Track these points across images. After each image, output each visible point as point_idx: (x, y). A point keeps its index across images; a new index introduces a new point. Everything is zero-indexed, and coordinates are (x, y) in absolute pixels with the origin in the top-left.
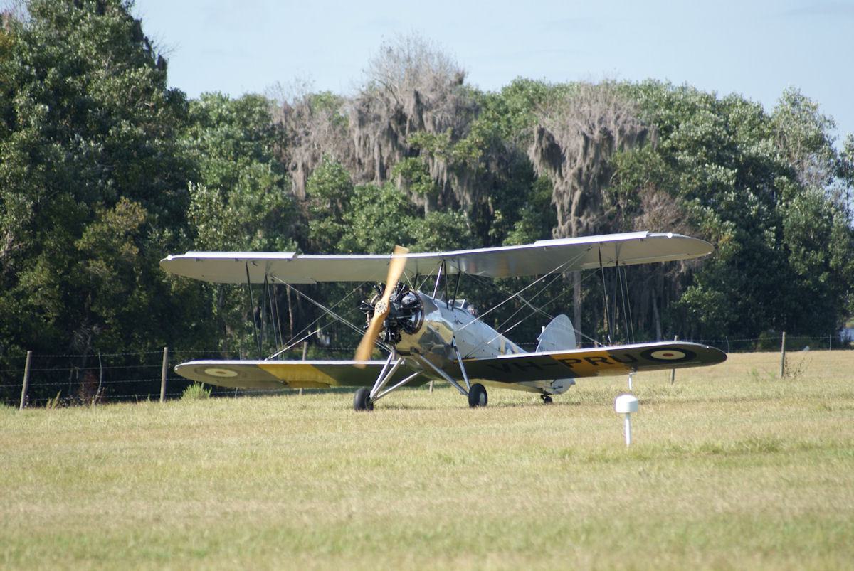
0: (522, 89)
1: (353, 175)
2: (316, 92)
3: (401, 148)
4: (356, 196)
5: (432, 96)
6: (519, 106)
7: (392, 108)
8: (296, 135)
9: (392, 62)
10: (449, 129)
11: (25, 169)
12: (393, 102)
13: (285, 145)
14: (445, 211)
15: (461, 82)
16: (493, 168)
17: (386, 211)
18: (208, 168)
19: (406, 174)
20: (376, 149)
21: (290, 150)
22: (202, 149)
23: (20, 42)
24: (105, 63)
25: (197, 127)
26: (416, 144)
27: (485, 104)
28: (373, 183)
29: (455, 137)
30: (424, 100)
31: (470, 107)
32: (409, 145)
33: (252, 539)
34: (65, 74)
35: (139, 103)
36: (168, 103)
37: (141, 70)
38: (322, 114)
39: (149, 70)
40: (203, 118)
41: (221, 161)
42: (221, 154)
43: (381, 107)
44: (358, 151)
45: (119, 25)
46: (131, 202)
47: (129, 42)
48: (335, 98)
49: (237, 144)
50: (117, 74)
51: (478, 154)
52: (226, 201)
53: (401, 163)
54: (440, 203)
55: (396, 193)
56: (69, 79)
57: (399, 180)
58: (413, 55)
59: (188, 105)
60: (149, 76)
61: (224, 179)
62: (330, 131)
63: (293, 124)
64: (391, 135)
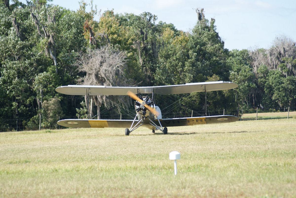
1: (269, 68)
2: (260, 48)
4: (269, 73)
5: (288, 49)
8: (255, 58)
10: (292, 57)
12: (278, 50)
13: (253, 61)
14: (291, 76)
15: (295, 45)
17: (277, 76)
18: (234, 67)
21: (253, 62)
22: (233, 63)
25: (231, 57)
26: (284, 60)
30: (286, 50)
32: (282, 60)
33: (245, 154)
35: (218, 52)
36: (224, 52)
39: (220, 44)
40: (233, 55)
41: (237, 65)
42: (237, 64)
44: (270, 62)
45: (213, 34)
47: (215, 38)
48: (264, 50)
49: (240, 61)
50: (212, 45)
52: (238, 74)
53: (280, 65)
55: (279, 72)
56: (202, 47)
57: (280, 69)
59: (229, 52)
60: (220, 46)
61: (238, 69)
62: (263, 57)
63: (254, 56)
64: (278, 58)
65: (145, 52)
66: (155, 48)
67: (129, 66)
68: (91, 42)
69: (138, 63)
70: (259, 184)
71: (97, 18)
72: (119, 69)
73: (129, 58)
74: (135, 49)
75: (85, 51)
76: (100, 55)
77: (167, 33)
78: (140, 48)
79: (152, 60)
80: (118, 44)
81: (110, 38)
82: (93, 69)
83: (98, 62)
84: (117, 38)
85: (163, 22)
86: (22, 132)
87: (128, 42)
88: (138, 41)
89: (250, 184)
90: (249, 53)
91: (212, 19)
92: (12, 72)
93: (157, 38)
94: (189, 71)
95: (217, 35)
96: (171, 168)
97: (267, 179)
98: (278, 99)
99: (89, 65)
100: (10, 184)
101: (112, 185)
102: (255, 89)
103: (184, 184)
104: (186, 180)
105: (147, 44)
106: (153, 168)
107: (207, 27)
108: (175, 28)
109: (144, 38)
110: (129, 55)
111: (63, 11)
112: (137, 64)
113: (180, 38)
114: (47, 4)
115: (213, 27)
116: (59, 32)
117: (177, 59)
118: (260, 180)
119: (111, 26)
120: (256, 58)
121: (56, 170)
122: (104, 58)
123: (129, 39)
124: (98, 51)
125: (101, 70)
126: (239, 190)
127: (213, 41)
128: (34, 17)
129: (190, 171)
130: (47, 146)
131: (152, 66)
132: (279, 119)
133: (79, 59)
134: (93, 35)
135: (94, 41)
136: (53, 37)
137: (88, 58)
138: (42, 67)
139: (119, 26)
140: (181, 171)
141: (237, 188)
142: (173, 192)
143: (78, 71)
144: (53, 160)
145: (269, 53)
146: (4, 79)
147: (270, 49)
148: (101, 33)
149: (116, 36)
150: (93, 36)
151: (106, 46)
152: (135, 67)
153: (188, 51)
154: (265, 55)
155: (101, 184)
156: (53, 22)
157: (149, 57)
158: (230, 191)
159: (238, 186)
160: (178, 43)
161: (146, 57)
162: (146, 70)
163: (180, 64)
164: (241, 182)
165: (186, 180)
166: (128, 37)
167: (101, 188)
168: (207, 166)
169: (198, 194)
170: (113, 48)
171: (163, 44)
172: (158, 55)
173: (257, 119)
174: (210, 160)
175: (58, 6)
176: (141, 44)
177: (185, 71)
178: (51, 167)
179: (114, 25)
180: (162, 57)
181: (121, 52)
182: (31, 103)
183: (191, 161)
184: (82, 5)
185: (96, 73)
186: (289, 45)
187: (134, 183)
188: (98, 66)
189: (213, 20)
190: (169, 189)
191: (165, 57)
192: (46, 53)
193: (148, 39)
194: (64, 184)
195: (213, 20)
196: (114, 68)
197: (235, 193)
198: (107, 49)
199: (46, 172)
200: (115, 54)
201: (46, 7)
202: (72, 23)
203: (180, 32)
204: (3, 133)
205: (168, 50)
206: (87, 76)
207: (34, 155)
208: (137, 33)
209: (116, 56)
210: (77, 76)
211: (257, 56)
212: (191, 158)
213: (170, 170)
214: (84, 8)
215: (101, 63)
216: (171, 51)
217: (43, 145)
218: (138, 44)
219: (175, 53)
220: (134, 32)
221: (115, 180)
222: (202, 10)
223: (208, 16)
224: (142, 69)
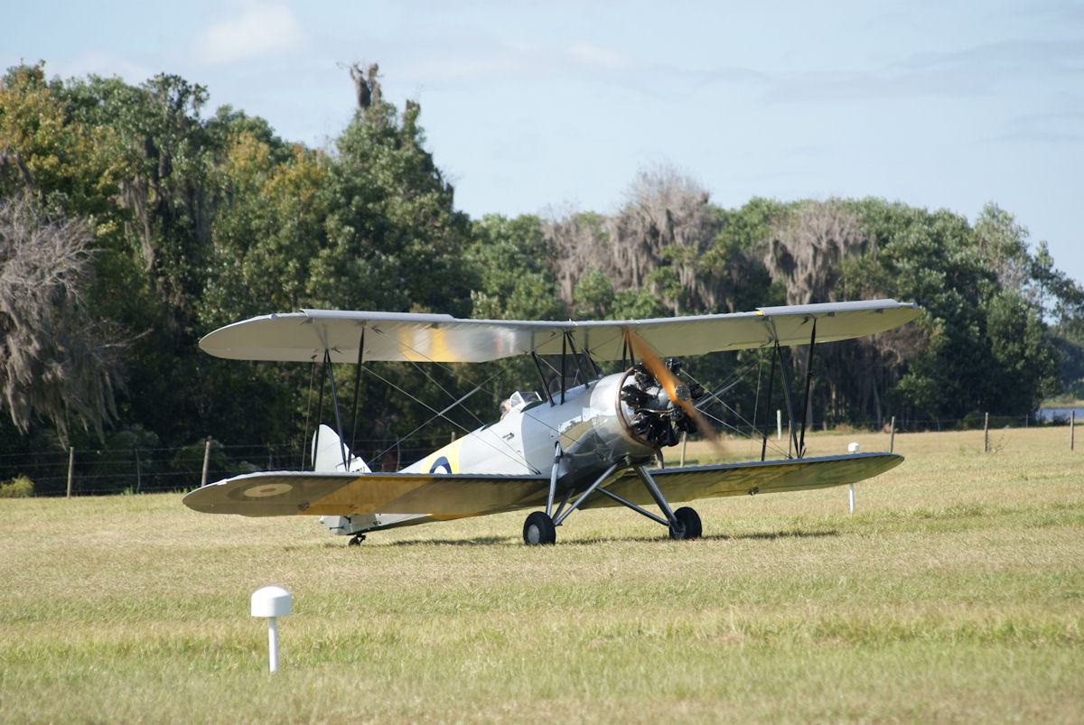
0: (757, 206)
1: (614, 283)
2: (581, 212)
3: (654, 258)
6: (756, 221)
8: (564, 248)
9: (647, 186)
10: (697, 243)
11: (332, 280)
12: (648, 219)
13: (556, 258)
15: (706, 201)
16: (735, 274)
19: (659, 281)
20: (634, 259)
21: (560, 262)
22: (485, 263)
23: (330, 174)
24: (400, 191)
25: (479, 244)
26: (668, 256)
27: (726, 219)
28: (631, 289)
29: (702, 249)
30: (674, 217)
31: (713, 222)
32: (662, 256)
33: (527, 596)
34: (367, 201)
35: (429, 224)
36: (453, 224)
37: (429, 195)
38: (587, 231)
40: (484, 236)
42: (499, 267)
43: (637, 224)
44: (620, 263)
45: (412, 157)
47: (421, 172)
48: (598, 216)
49: (512, 257)
50: (410, 200)
51: (721, 263)
53: (655, 272)
54: (688, 305)
55: (652, 297)
56: (370, 206)
57: (653, 287)
58: (665, 178)
59: (471, 225)
60: (437, 200)
61: (502, 287)
63: (562, 239)
64: (647, 248)
65: (164, 222)
66: (201, 205)
67: (100, 274)
69: (136, 260)
72: (64, 281)
73: (102, 242)
74: (123, 210)
77: (243, 152)
78: (145, 205)
79: (187, 251)
80: (60, 191)
84: (57, 167)
85: (235, 110)
87: (98, 183)
88: (136, 179)
89: (543, 703)
90: (543, 230)
91: (408, 102)
93: (206, 170)
95: (427, 163)
96: (258, 647)
101: (31, 710)
103: (303, 706)
104: (309, 693)
105: (169, 193)
106: (190, 649)
107: (390, 132)
108: (275, 135)
109: (160, 169)
110: (102, 230)
112: (133, 265)
113: (293, 171)
115: (413, 131)
117: (280, 248)
119: (36, 125)
123: (104, 170)
127: (412, 184)
131: (189, 271)
139: (66, 123)
145: (616, 229)
147: (620, 215)
149: (52, 160)
151: (15, 199)
152: (126, 276)
153: (322, 219)
157: (177, 241)
159: (501, 711)
160: (286, 191)
161: (165, 240)
162: (168, 287)
163: (293, 265)
164: (510, 697)
166: (100, 166)
168: (391, 639)
170: (40, 205)
171: (230, 194)
172: (211, 233)
174: (402, 617)
176: (147, 192)
177: (308, 291)
179: (49, 121)
180: (224, 239)
181: (72, 221)
186: (685, 204)
189: (413, 109)
191: (238, 241)
193: (176, 175)
195: (414, 105)
196: (48, 281)
198: (18, 208)
200: (50, 228)
205: (246, 215)
208: (134, 152)
209: (52, 234)
211: (571, 241)
216: (260, 217)
218: (136, 190)
219: (273, 227)
220: (122, 148)
221: (45, 694)
223: (394, 94)
224: (153, 284)
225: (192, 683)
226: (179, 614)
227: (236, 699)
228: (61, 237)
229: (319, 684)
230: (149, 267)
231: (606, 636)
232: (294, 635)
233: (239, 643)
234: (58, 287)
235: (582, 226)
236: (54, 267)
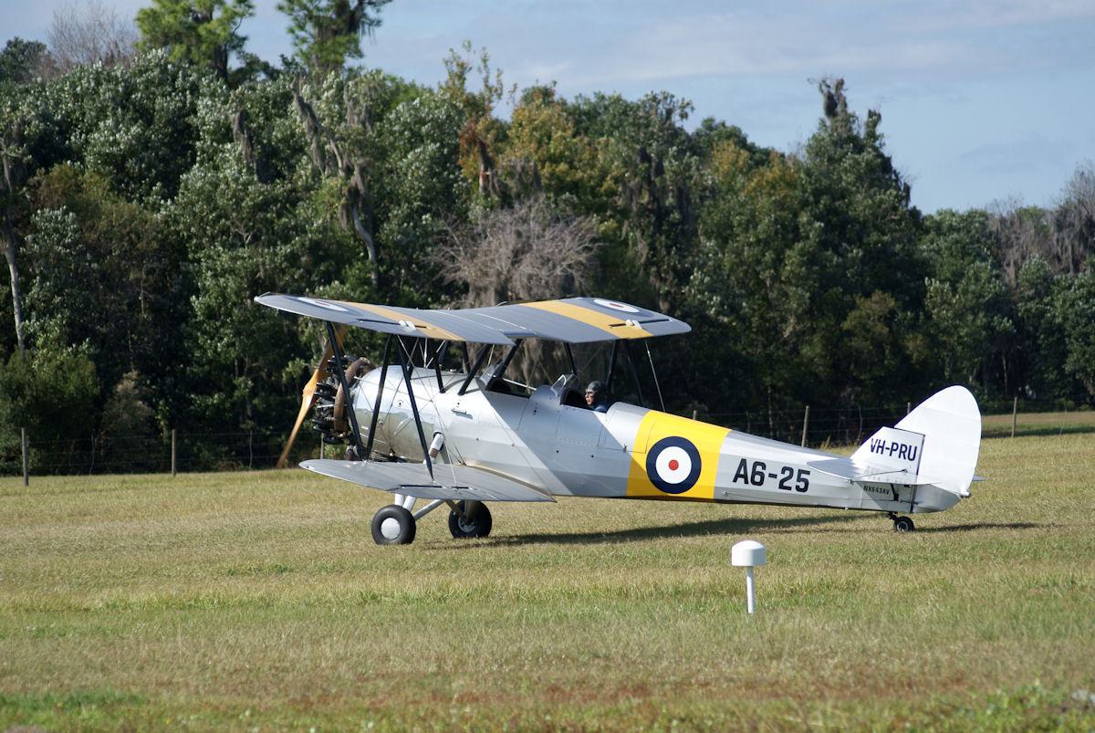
2: (1025, 207)
7: (1084, 217)
11: (803, 269)
12: (1085, 213)
20: (1070, 248)
22: (938, 252)
33: (973, 548)
34: (834, 199)
38: (1029, 224)
41: (952, 260)
46: (883, 293)
48: (1040, 210)
49: (963, 248)
52: (955, 291)
61: (954, 274)
67: (604, 265)
68: (485, 189)
70: (1016, 644)
71: (503, 111)
72: (573, 272)
73: (604, 237)
75: (463, 217)
76: (514, 229)
77: (725, 155)
80: (571, 193)
81: (546, 171)
82: (491, 271)
83: (505, 251)
84: (567, 173)
85: (718, 121)
86: (265, 473)
89: (986, 645)
91: (870, 111)
92: (231, 284)
94: (800, 280)
95: (886, 164)
96: (737, 592)
97: (1039, 630)
98: (1083, 369)
99: (481, 259)
100: (232, 642)
101: (546, 644)
102: (1008, 337)
103: (777, 645)
104: (782, 633)
106: (680, 593)
107: (854, 139)
108: (749, 141)
111: (398, 88)
113: (770, 174)
114: (346, 65)
115: (872, 135)
116: (382, 154)
117: (758, 241)
118: (1018, 631)
120: (1013, 236)
121: (374, 597)
122: (524, 239)
124: (504, 217)
125: (516, 276)
126: (951, 665)
128: (306, 108)
129: (797, 602)
130: (344, 518)
132: (1087, 435)
133: (445, 242)
134: (489, 163)
135: (493, 185)
136: (363, 171)
137: (475, 238)
138: (327, 268)
139: (574, 136)
140: (769, 603)
141: (945, 658)
142: (741, 669)
143: (442, 278)
144: (365, 565)
146: (209, 306)
147: (1058, 209)
148: (512, 157)
149: (563, 166)
150: (492, 169)
151: (532, 201)
153: (796, 215)
154: (1041, 231)
155: (513, 642)
156: (364, 124)
158: (922, 667)
159: (948, 651)
160: (764, 191)
163: (769, 256)
164: (957, 638)
165: (782, 633)
167: (516, 656)
168: (852, 587)
169: (822, 677)
170: (553, 206)
173: (1017, 435)
174: (863, 568)
175: (378, 72)
177: (783, 278)
178: (356, 586)
179: (560, 133)
181: (579, 219)
182: (293, 379)
183: (802, 569)
184: (456, 69)
185: (499, 288)
187: (617, 639)
188: (503, 264)
189: (875, 118)
190: (729, 662)
192: (344, 223)
193: (668, 176)
194: (399, 641)
195: (875, 114)
196: (558, 271)
197: (939, 674)
198: (533, 210)
199: (342, 602)
200: (561, 225)
201: (343, 76)
202: (424, 129)
203: (767, 153)
204: (207, 475)
206: (471, 295)
207: (303, 549)
209: (562, 231)
210: (443, 297)
211: (1015, 232)
212: (799, 559)
213: (734, 598)
214: (461, 77)
215: (517, 257)
216: (740, 214)
217: (332, 515)
219: (752, 222)
221: (558, 630)
222: (840, 84)
223: (858, 105)
225: (681, 623)
226: (669, 562)
227: (720, 637)
228: (571, 233)
229: (789, 626)
230: (643, 260)
231: (1043, 586)
232: (772, 580)
233: (722, 589)
234: (567, 276)
235: (1025, 218)
236: (564, 260)
